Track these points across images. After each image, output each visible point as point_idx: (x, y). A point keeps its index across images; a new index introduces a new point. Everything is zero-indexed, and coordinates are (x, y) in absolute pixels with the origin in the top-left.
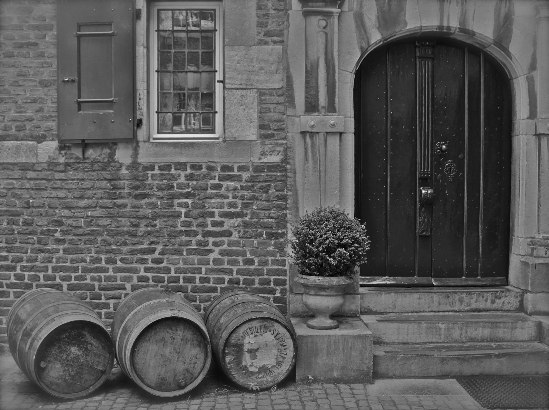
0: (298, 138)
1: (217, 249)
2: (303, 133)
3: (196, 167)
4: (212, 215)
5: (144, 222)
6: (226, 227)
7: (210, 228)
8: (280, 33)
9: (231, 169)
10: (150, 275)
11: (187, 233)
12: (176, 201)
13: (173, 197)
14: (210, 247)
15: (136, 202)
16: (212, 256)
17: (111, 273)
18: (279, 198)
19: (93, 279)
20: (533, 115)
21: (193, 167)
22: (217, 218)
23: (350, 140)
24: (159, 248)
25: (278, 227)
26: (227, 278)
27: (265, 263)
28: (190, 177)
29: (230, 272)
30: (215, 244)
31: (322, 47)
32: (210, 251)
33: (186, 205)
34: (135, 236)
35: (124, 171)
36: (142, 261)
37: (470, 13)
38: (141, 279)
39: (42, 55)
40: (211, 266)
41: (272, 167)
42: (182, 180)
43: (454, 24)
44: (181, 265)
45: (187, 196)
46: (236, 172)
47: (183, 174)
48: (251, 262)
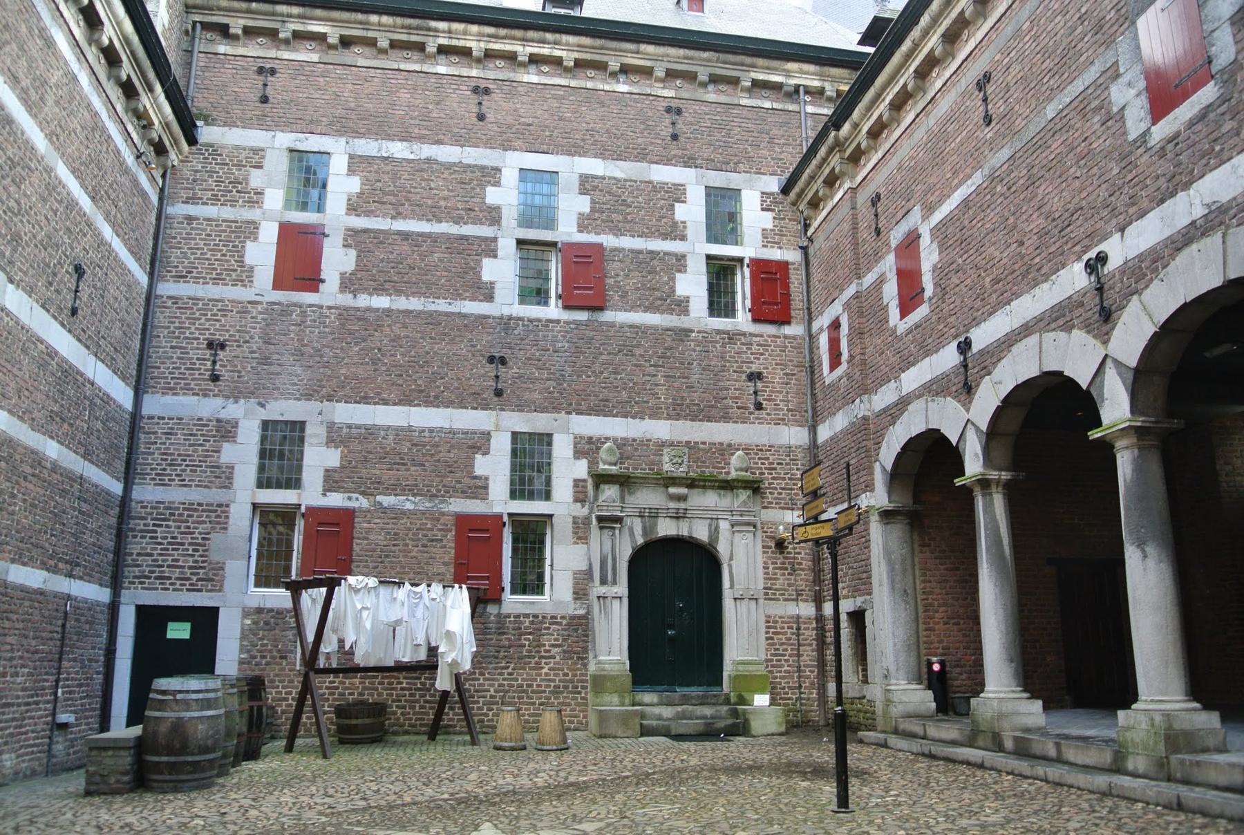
0: (595, 600)
1: (547, 667)
2: (599, 597)
3: (536, 616)
4: (544, 645)
5: (503, 650)
6: (552, 653)
7: (543, 654)
8: (586, 538)
9: (556, 618)
10: (505, 682)
11: (529, 657)
12: (523, 637)
13: (521, 635)
14: (543, 665)
15: (499, 637)
16: (544, 671)
17: (481, 681)
18: (584, 636)
19: (470, 685)
20: (732, 586)
21: (533, 616)
22: (547, 648)
23: (626, 601)
24: (512, 665)
25: (583, 653)
26: (553, 684)
27: (576, 675)
28: (532, 623)
29: (554, 681)
30: (546, 663)
31: (610, 546)
32: (542, 668)
33: (529, 639)
34: (497, 658)
35: (492, 618)
36: (500, 674)
37: (694, 528)
38: (500, 685)
39: (445, 547)
40: (543, 677)
41: (580, 617)
42: (527, 624)
43: (686, 533)
44: (525, 676)
45: (530, 634)
46: (559, 620)
47: (527, 620)
48: (567, 675)
